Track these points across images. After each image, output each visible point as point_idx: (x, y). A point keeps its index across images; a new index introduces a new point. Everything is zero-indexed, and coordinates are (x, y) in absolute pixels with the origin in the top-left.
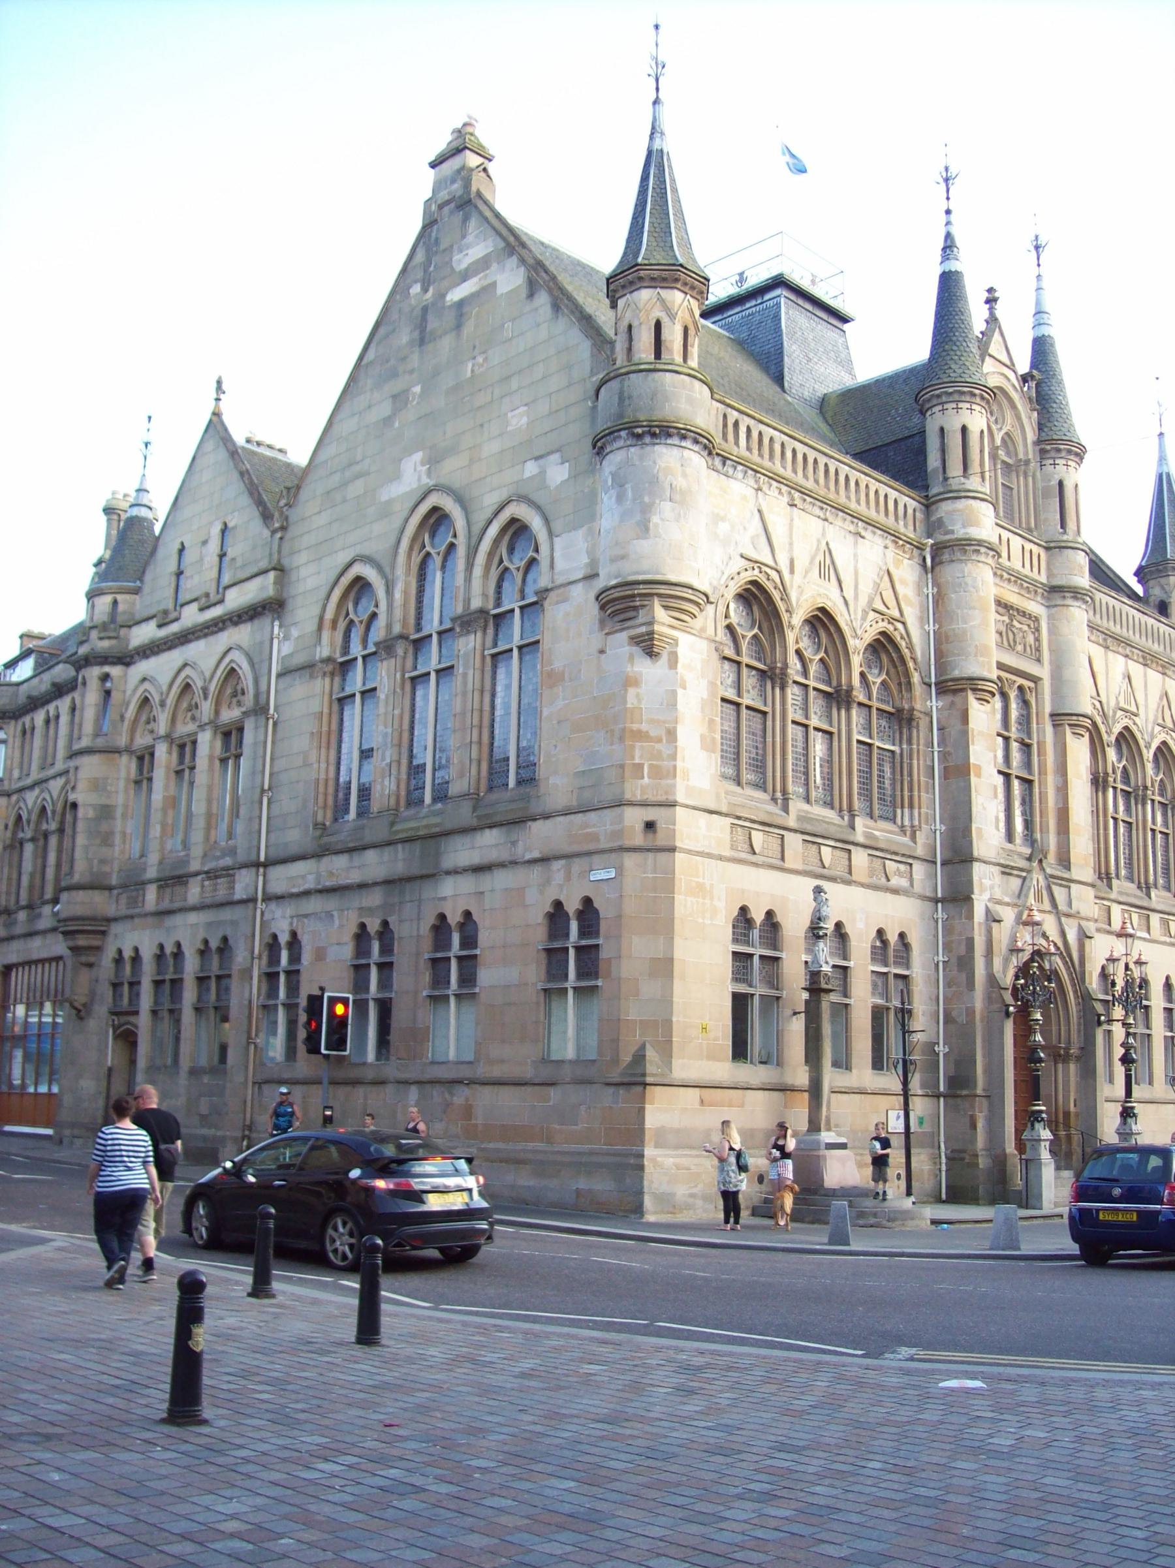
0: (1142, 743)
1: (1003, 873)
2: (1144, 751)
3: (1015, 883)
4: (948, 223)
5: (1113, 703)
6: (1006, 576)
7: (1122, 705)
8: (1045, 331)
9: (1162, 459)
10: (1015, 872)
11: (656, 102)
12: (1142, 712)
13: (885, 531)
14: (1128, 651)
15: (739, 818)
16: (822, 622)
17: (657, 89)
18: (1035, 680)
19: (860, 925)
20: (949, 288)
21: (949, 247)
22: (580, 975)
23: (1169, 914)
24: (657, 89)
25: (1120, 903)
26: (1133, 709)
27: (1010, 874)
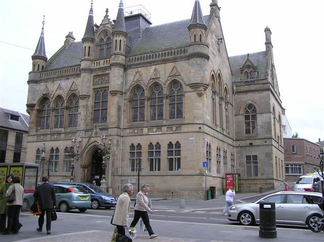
0: (162, 84)
2: (163, 86)
3: (90, 133)
4: (92, 6)
5: (149, 79)
7: (153, 77)
8: (122, 7)
11: (43, 28)
12: (162, 76)
13: (72, 75)
14: (156, 63)
16: (60, 97)
18: (108, 87)
19: (62, 147)
20: (91, 19)
21: (91, 10)
22: (55, 159)
26: (158, 77)
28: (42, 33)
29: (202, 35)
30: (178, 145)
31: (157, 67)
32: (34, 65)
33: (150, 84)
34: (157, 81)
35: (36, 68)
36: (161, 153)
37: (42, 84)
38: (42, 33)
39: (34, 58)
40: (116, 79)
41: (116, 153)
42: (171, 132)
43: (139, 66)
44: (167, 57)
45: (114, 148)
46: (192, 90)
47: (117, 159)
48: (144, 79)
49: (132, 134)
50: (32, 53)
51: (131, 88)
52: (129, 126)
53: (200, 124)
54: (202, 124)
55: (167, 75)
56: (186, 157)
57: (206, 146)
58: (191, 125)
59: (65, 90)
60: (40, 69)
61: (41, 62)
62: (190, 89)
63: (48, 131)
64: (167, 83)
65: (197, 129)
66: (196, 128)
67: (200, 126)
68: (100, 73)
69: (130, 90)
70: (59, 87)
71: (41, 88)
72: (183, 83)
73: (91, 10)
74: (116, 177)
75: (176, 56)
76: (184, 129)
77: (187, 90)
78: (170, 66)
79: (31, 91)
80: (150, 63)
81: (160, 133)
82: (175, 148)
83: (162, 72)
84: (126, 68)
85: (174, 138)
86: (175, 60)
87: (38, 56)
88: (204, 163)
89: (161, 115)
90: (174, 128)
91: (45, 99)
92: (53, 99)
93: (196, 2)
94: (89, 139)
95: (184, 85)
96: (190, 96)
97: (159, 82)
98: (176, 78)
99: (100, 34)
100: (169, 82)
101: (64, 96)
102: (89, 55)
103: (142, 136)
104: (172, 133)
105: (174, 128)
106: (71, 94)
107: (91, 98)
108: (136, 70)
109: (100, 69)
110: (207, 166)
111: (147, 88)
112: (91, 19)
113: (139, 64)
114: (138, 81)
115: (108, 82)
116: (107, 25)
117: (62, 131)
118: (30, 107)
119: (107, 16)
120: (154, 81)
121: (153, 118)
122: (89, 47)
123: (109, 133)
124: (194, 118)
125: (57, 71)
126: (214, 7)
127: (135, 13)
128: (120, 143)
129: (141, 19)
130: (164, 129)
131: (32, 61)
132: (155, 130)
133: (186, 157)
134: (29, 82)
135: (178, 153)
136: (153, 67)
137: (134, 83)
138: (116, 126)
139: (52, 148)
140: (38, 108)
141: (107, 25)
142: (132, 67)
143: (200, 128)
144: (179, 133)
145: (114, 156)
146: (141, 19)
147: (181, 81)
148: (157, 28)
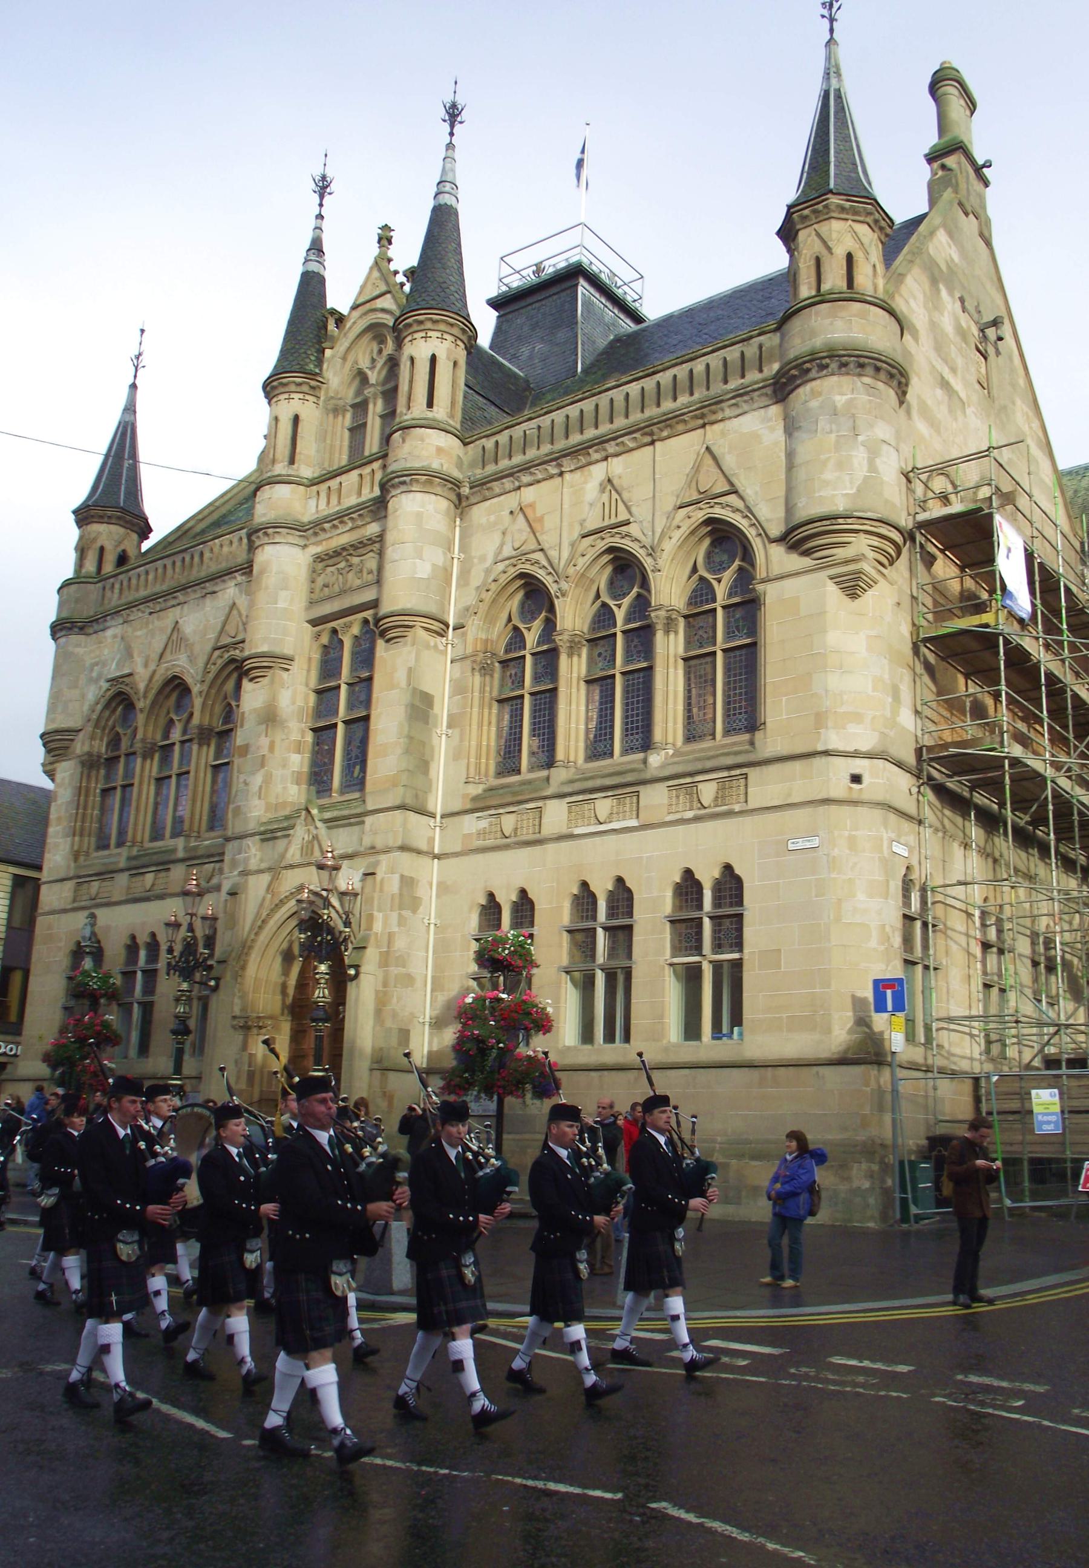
1: (263, 840)
4: (318, 228)
6: (327, 526)
8: (446, 199)
9: (832, 70)
10: (279, 834)
11: (134, 387)
12: (641, 512)
15: (79, 877)
16: (176, 687)
17: (135, 376)
20: (311, 287)
21: (316, 247)
23: (691, 774)
24: (135, 376)
25: (561, 796)
26: (623, 516)
27: (276, 838)
28: (130, 408)
29: (859, 256)
30: (730, 885)
31: (617, 466)
32: (82, 550)
33: (582, 562)
34: (617, 541)
35: (90, 567)
36: (637, 938)
37: (109, 633)
38: (130, 408)
39: (84, 515)
40: (431, 555)
41: (400, 944)
42: (690, 814)
43: (526, 479)
44: (668, 405)
45: (381, 922)
46: (807, 562)
47: (408, 980)
48: (548, 540)
49: (489, 843)
50: (80, 493)
51: (488, 597)
52: (475, 799)
53: (855, 755)
54: (870, 756)
55: (668, 503)
56: (772, 957)
57: (896, 885)
58: (797, 766)
59: (197, 649)
60: (109, 567)
61: (108, 534)
62: (796, 562)
63: (120, 856)
64: (669, 546)
65: (840, 787)
66: (833, 777)
67: (859, 766)
68: (344, 539)
69: (483, 608)
70: (176, 638)
71: (108, 653)
72: (751, 533)
73: (316, 247)
74: (391, 1075)
75: (717, 388)
76: (765, 786)
77: (776, 571)
78: (679, 451)
79: (63, 669)
80: (582, 449)
81: (634, 823)
82: (712, 910)
83: (639, 495)
84: (462, 497)
85: (705, 849)
86: (704, 415)
87: (114, 500)
88: (880, 986)
89: (642, 734)
90: (708, 791)
91: (120, 699)
92: (148, 702)
93: (826, 94)
94: (275, 878)
95: (757, 544)
96: (793, 593)
97: (627, 544)
98: (718, 512)
99: (349, 349)
100: (677, 535)
101: (192, 674)
102: (292, 461)
103: (537, 850)
104: (697, 819)
105: (708, 791)
106: (220, 662)
107: (295, 667)
108: (511, 501)
109: (340, 517)
110: (899, 1006)
111: (564, 585)
112: (311, 287)
113: (526, 468)
114: (521, 555)
115: (379, 582)
116: (380, 303)
117: (174, 850)
118: (56, 743)
119: (382, 262)
120: (601, 545)
121: (599, 745)
122: (296, 419)
123: (367, 841)
124: (820, 720)
125: (168, 562)
126: (951, 161)
127: (555, 264)
128: (421, 892)
129: (583, 289)
130: (655, 798)
131: (73, 533)
132: (604, 806)
133: (772, 957)
134: (59, 629)
135: (731, 930)
136: (598, 472)
137: (501, 567)
138: (397, 802)
139: (133, 937)
140: (86, 748)
141: (380, 303)
142: (496, 487)
143: (856, 779)
144: (730, 814)
145: (385, 960)
146: (583, 289)
147: (743, 524)
148: (668, 322)
